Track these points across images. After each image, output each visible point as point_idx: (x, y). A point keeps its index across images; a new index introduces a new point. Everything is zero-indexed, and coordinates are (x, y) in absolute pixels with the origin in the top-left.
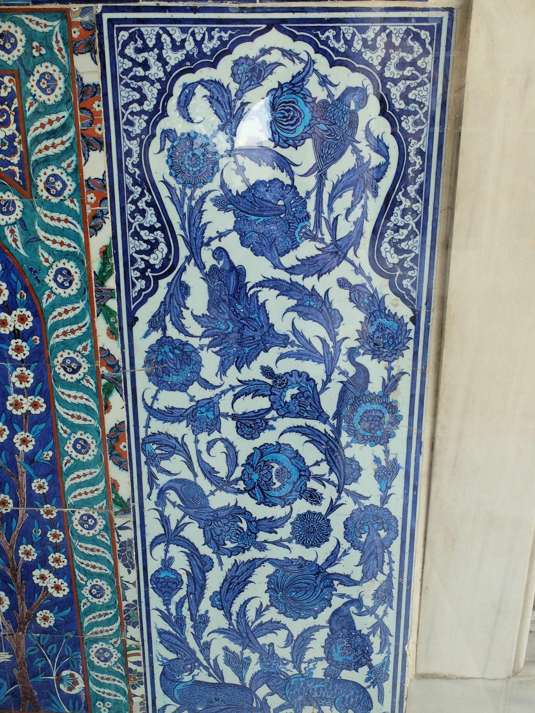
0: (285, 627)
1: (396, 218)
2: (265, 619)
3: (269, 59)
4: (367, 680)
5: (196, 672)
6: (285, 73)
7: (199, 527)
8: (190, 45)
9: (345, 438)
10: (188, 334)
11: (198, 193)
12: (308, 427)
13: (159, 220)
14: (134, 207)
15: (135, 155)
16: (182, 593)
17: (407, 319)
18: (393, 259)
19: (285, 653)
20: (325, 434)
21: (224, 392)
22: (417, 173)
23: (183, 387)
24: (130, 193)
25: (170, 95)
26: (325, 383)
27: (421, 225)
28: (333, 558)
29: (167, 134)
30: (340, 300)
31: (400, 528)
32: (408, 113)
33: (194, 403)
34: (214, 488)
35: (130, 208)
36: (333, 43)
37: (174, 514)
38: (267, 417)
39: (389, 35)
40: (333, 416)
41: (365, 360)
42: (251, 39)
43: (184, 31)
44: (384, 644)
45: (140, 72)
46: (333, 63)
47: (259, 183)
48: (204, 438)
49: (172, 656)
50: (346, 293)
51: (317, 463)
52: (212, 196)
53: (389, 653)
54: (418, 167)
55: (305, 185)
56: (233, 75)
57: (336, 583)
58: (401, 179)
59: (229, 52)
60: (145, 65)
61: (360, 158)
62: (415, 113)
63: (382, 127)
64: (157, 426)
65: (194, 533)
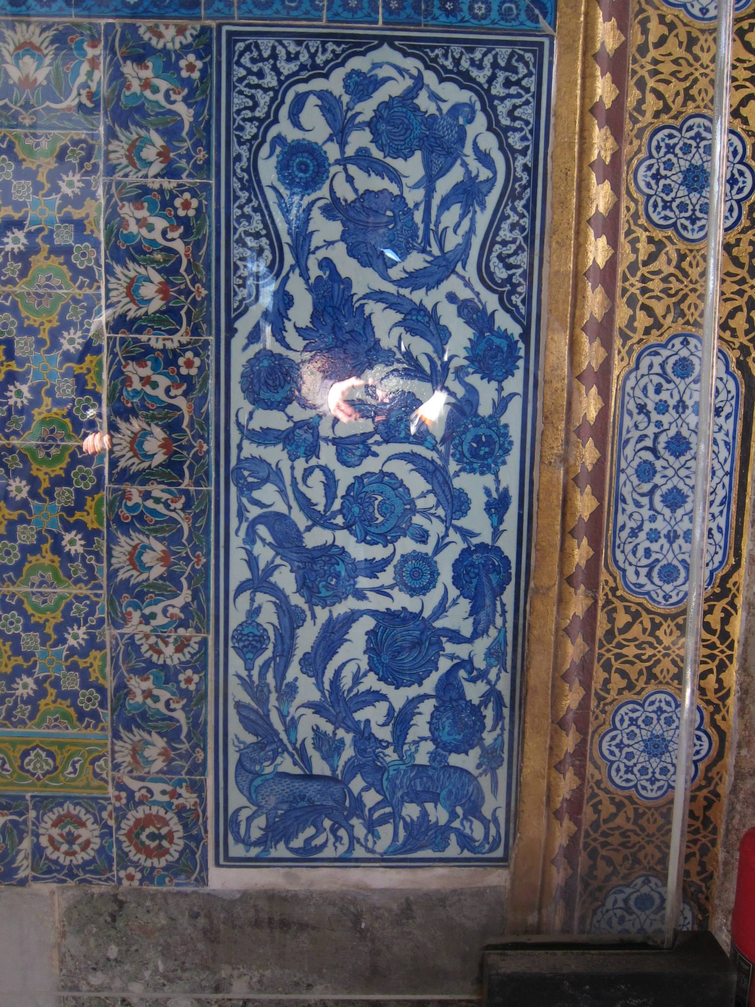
0: (384, 698)
1: (505, 233)
2: (362, 688)
3: (381, 73)
4: (479, 766)
5: (279, 760)
6: (396, 88)
8: (304, 58)
9: (453, 467)
10: (288, 347)
11: (307, 200)
12: (414, 454)
13: (266, 226)
14: (239, 212)
15: (245, 159)
16: (268, 654)
17: (516, 337)
18: (501, 273)
19: (384, 734)
20: (432, 462)
22: (524, 188)
23: (282, 405)
24: (237, 198)
25: (282, 102)
27: (529, 239)
28: (441, 609)
29: (280, 139)
30: (449, 315)
31: (513, 571)
32: (515, 130)
33: (291, 424)
34: (310, 523)
35: (236, 212)
36: (441, 61)
37: (264, 554)
38: (370, 441)
39: (495, 57)
41: (474, 380)
42: (363, 54)
43: (299, 43)
44: (499, 717)
45: (254, 80)
46: (442, 80)
47: (367, 192)
48: (301, 465)
49: (250, 739)
50: (453, 308)
51: (423, 495)
52: (321, 203)
53: (503, 729)
54: (524, 182)
55: (414, 196)
56: (346, 87)
57: (444, 639)
58: (509, 195)
59: (342, 64)
60: (260, 75)
61: (468, 172)
62: (521, 130)
63: (489, 143)
64: (250, 449)
65: (285, 579)
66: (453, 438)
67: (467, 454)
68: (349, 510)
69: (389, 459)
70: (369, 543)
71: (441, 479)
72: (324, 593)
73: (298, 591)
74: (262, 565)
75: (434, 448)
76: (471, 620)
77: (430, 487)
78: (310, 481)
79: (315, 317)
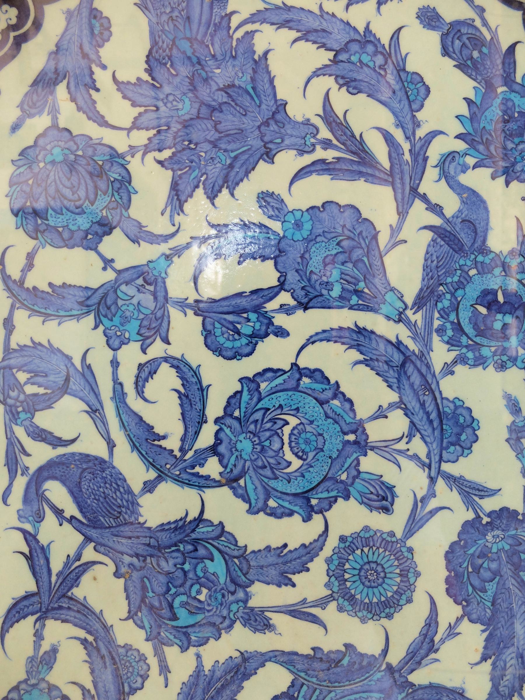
7: (117, 574)
9: (440, 354)
20: (398, 345)
21: (178, 251)
26: (395, 230)
33: (110, 275)
34: (152, 474)
40: (415, 304)
50: (433, 38)
51: (381, 414)
65: (104, 590)
66: (440, 298)
67: (468, 329)
68: (233, 448)
69: (311, 341)
70: (273, 514)
71: (416, 379)
72: (184, 618)
73: (131, 616)
74: (57, 564)
75: (401, 318)
76: (487, 666)
77: (393, 397)
78: (150, 389)
79: (153, 61)
